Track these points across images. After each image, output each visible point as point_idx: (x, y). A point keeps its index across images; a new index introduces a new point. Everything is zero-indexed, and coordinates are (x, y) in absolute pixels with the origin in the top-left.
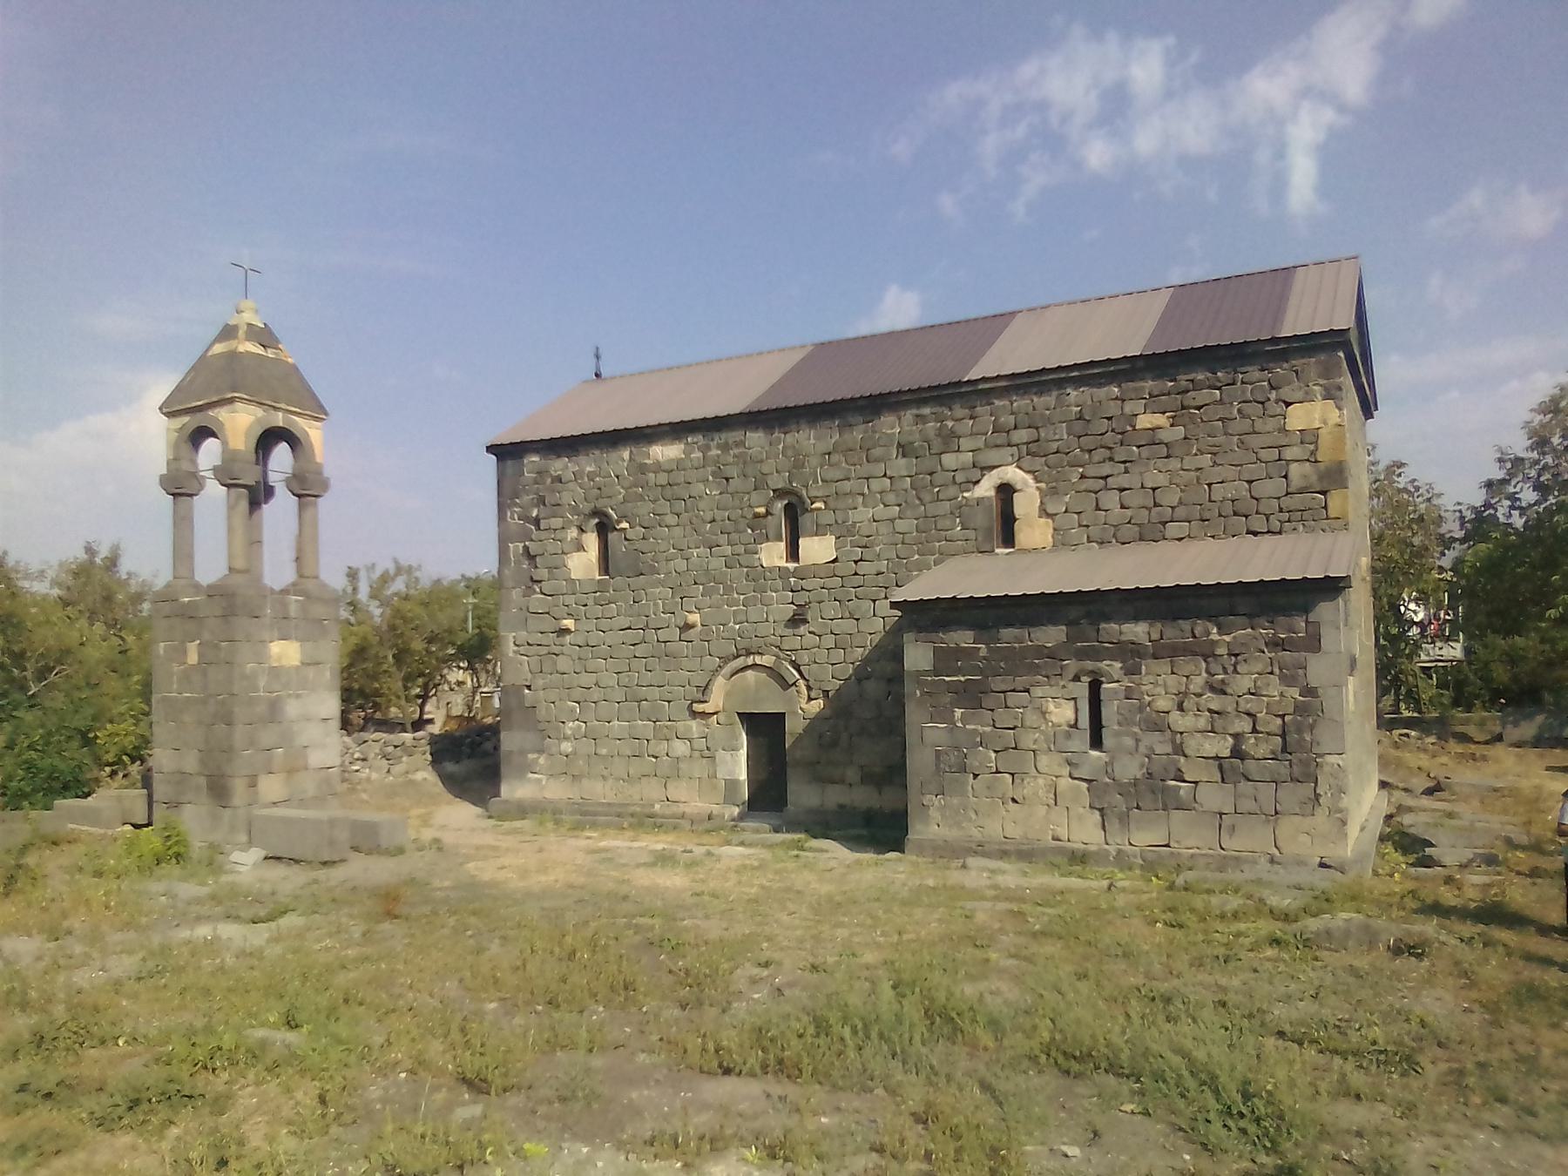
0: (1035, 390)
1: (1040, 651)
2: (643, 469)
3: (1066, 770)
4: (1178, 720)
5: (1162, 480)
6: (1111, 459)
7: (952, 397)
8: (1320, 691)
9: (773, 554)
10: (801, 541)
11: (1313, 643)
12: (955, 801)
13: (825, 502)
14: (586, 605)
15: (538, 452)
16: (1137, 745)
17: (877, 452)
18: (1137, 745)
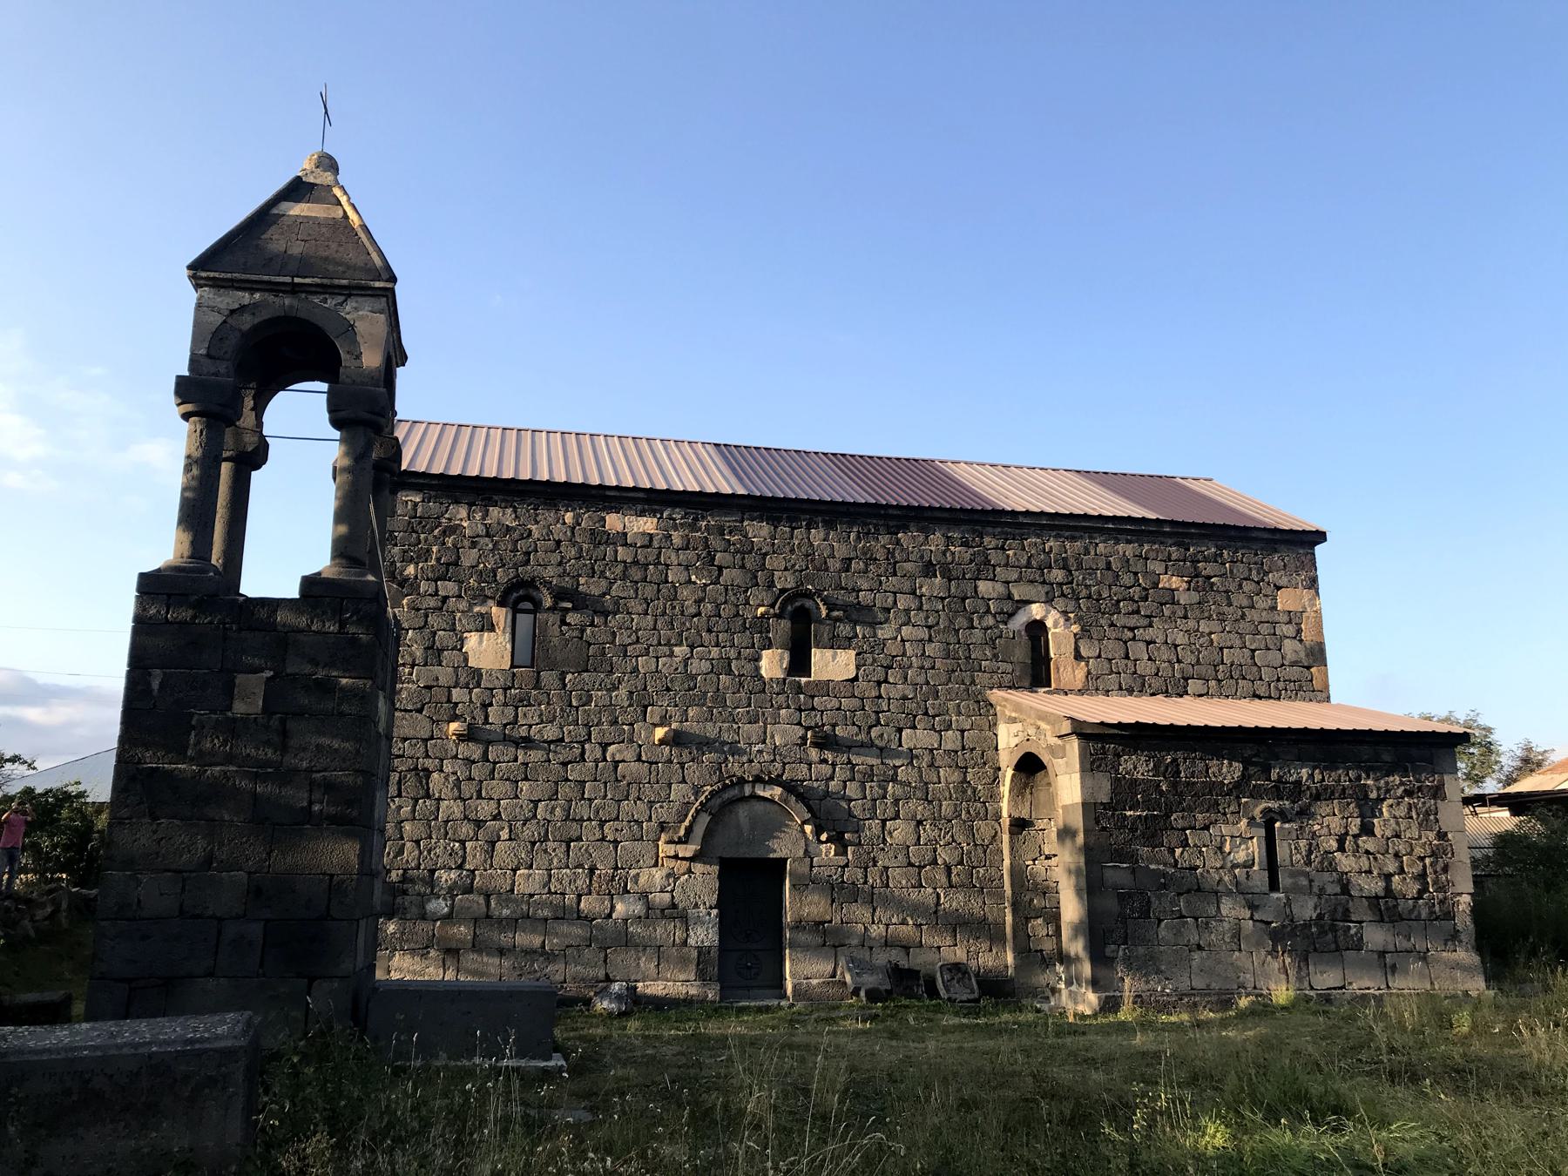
0: (1067, 534)
1: (1214, 787)
2: (600, 538)
3: (1248, 914)
4: (1345, 862)
5: (1181, 639)
6: (1138, 612)
7: (989, 524)
8: (1450, 836)
9: (772, 664)
10: (818, 656)
11: (1438, 792)
12: (1141, 950)
13: (845, 611)
14: (491, 704)
15: (421, 491)
16: (1311, 886)
17: (908, 566)
18: (1311, 886)
